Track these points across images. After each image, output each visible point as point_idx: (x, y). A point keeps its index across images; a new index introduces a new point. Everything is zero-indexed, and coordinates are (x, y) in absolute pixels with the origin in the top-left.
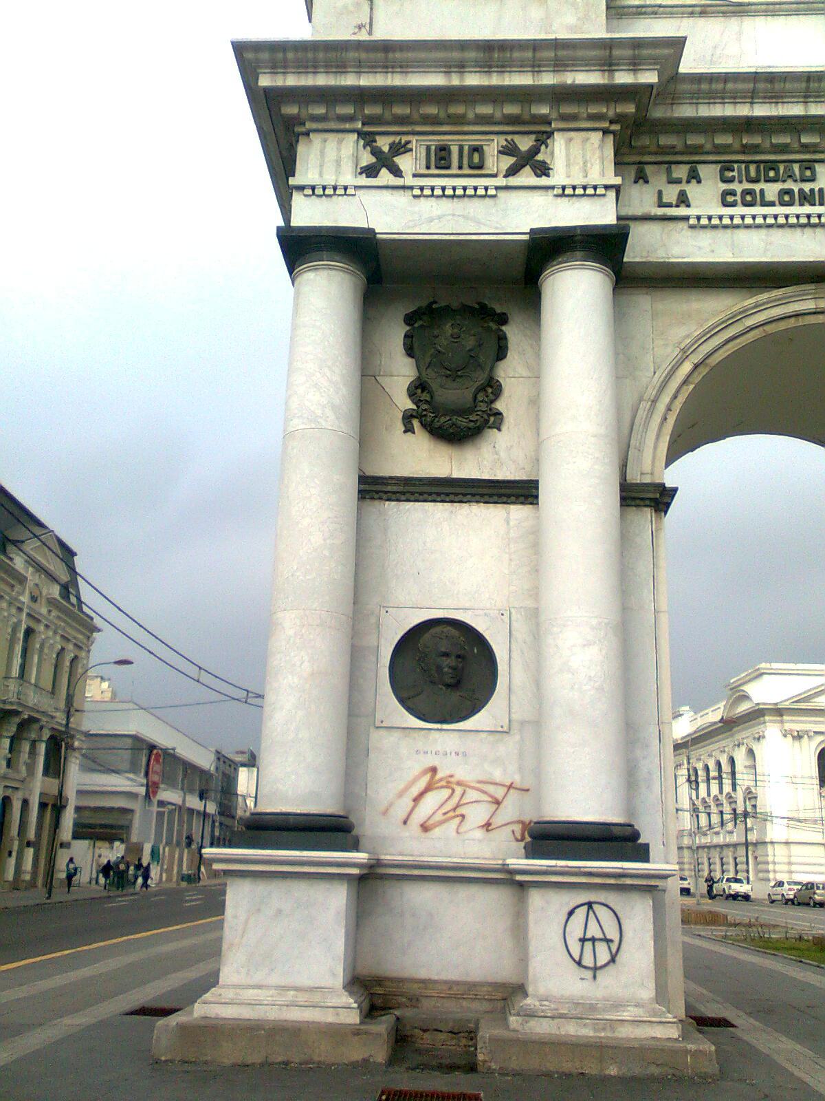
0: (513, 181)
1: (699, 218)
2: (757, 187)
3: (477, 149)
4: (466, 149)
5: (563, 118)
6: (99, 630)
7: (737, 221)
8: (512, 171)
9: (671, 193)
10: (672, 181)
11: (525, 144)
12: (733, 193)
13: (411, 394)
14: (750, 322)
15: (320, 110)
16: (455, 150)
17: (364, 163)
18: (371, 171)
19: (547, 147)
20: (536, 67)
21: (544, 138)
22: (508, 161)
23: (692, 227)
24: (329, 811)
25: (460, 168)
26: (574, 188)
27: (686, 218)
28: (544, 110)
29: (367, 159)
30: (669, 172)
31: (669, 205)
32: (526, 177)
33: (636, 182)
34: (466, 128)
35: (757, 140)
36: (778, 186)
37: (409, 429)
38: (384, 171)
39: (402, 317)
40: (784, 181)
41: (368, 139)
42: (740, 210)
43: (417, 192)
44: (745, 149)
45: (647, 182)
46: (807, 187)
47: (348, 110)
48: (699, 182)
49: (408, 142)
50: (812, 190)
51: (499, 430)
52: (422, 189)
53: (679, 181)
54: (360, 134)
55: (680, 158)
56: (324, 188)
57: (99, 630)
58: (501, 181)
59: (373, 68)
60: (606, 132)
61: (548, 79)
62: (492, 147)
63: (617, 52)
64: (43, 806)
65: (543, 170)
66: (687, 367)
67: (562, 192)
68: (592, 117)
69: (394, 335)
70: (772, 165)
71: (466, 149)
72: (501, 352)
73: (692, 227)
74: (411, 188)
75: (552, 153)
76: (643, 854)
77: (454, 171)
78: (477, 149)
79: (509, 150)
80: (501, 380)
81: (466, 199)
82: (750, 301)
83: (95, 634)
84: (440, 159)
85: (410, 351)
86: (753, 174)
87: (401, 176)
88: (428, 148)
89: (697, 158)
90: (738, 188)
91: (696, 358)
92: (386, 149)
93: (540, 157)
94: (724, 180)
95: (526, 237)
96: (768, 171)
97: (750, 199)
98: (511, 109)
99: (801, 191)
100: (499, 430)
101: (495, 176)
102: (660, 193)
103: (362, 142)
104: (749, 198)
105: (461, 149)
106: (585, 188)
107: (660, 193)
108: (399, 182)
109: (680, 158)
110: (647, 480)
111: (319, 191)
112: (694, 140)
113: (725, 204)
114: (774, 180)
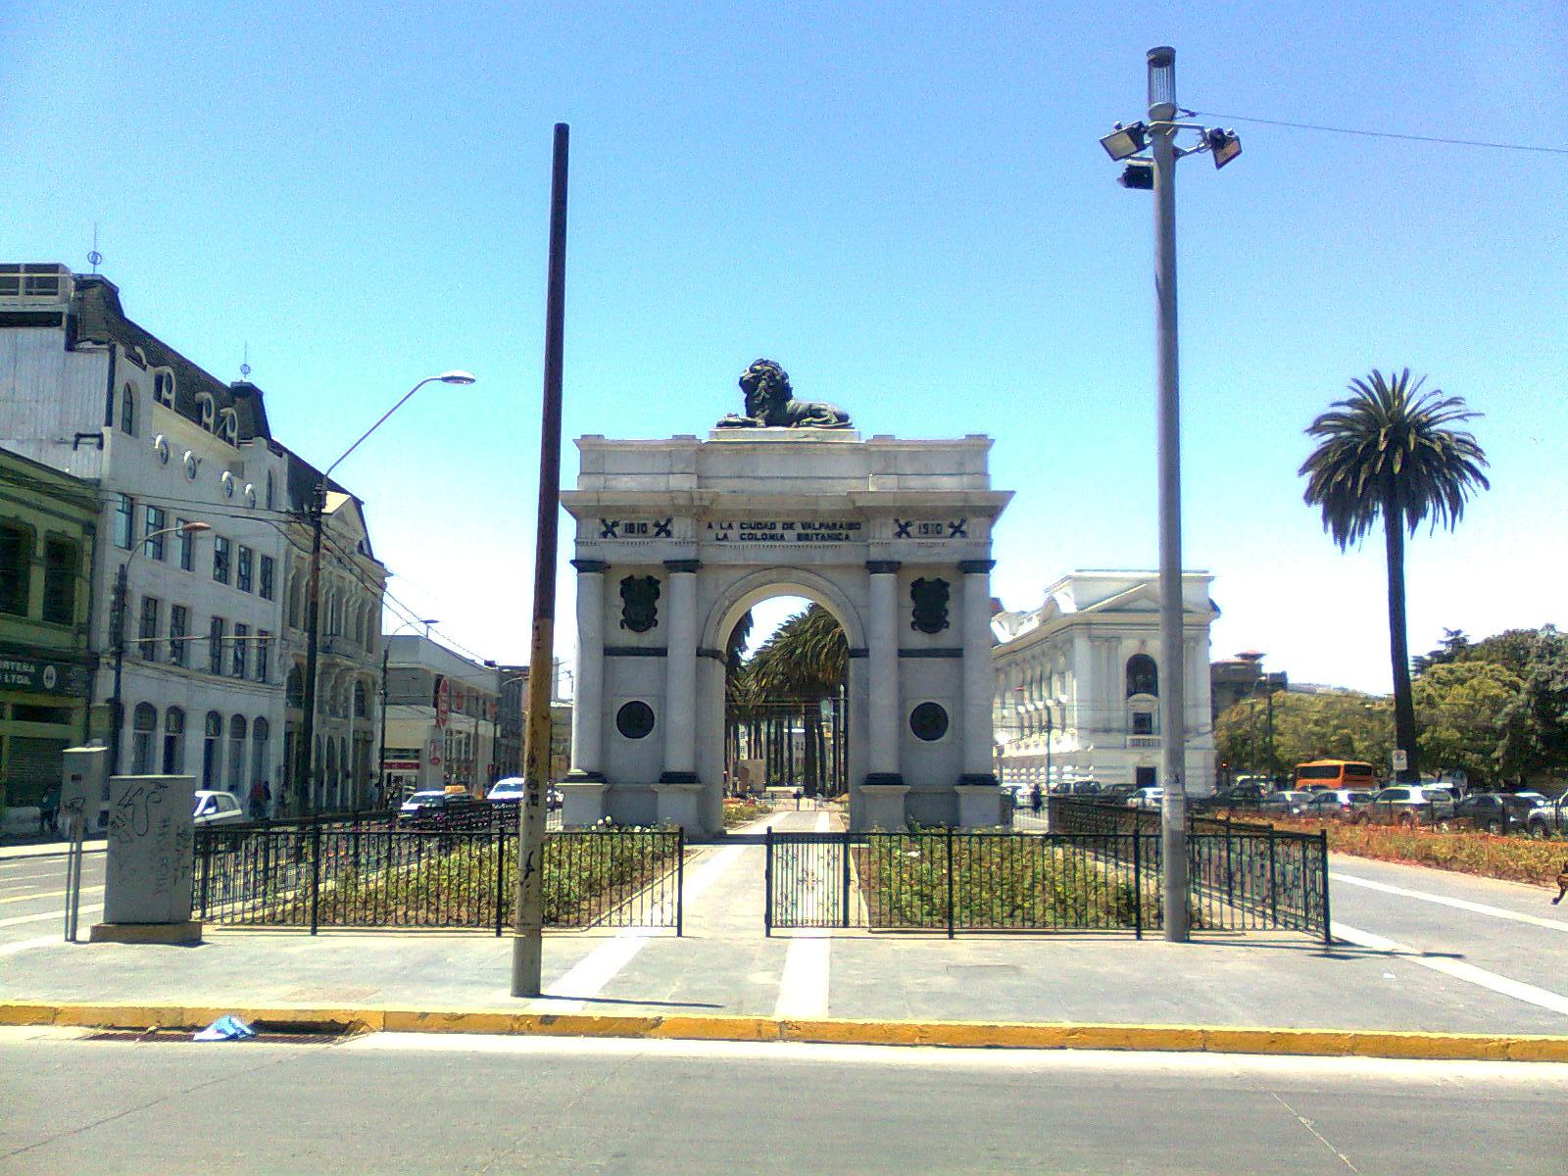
2: (753, 532)
3: (645, 525)
6: (390, 575)
10: (722, 528)
13: (623, 613)
16: (636, 526)
18: (605, 535)
36: (762, 531)
37: (622, 627)
38: (609, 535)
46: (773, 532)
57: (390, 575)
64: (356, 741)
65: (669, 534)
72: (657, 594)
75: (672, 527)
90: (746, 531)
93: (669, 528)
94: (742, 528)
97: (752, 537)
114: (761, 528)
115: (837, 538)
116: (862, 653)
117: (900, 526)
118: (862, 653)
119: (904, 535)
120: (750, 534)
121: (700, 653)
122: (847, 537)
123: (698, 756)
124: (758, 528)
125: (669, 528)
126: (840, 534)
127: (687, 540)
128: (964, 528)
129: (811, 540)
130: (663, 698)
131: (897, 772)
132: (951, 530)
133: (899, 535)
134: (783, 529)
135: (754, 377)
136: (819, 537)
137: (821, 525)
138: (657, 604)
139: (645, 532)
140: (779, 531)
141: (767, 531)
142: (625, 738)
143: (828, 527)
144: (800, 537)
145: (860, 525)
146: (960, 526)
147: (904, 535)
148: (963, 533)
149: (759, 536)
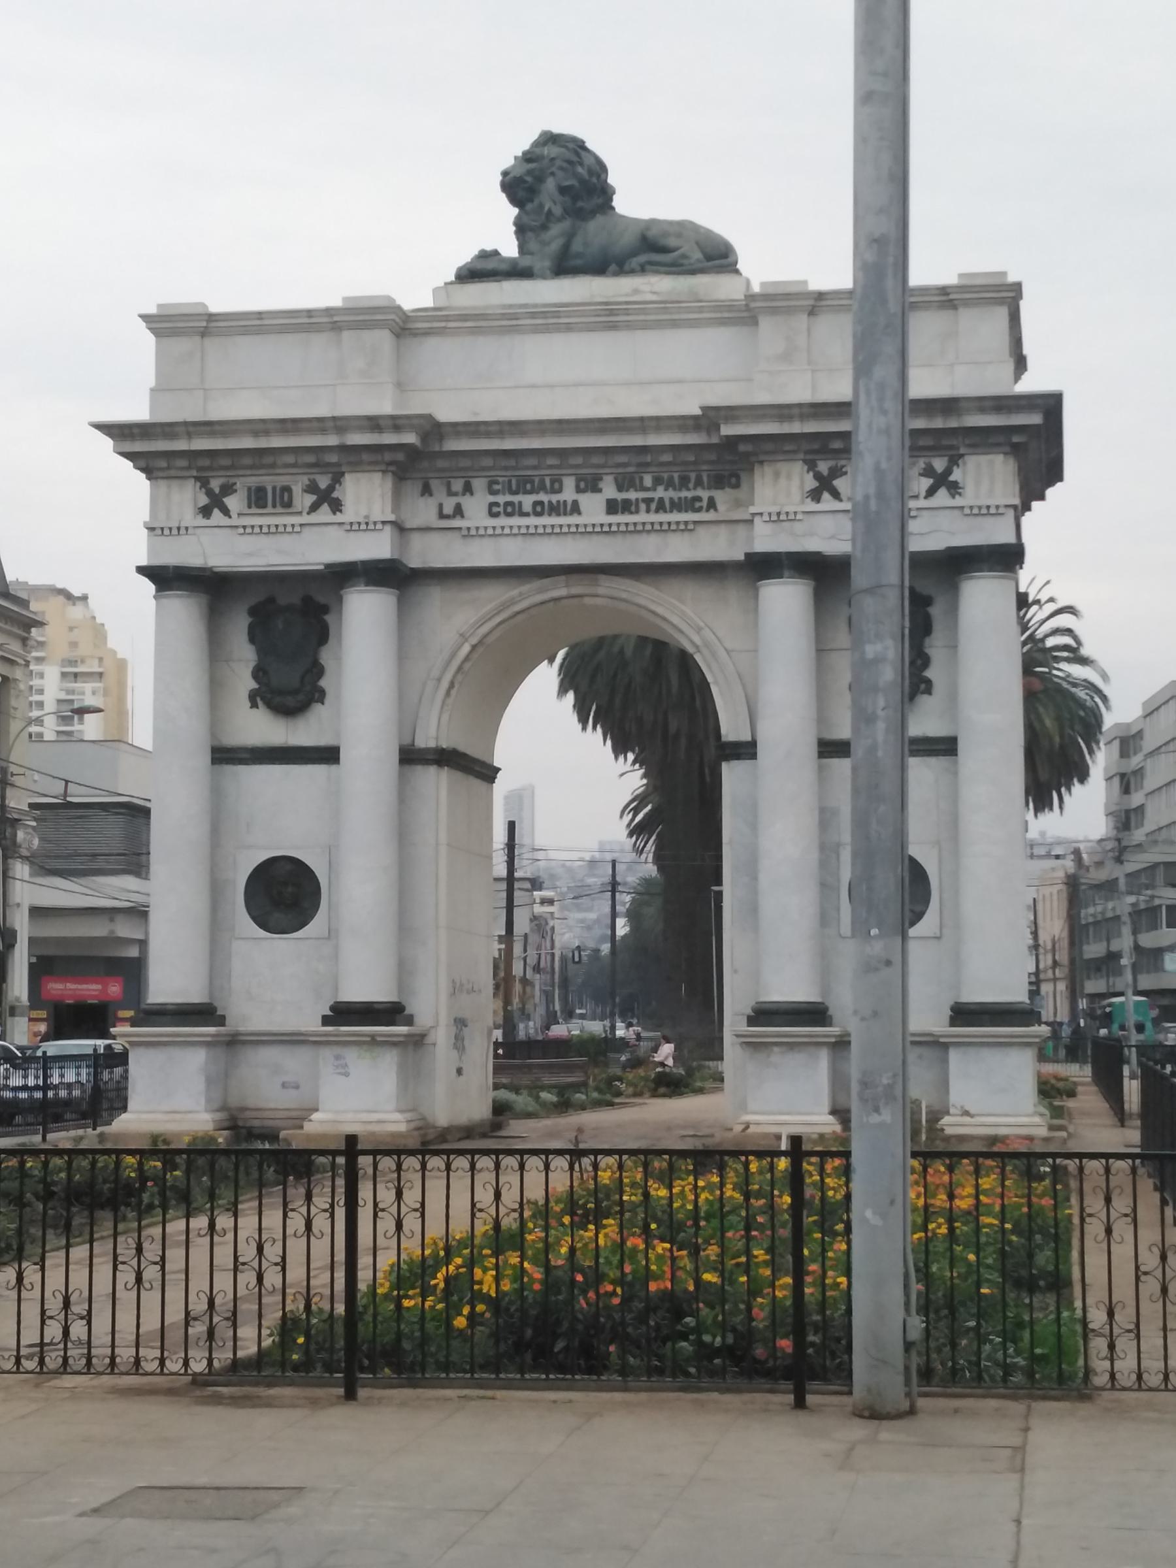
0: (315, 518)
1: (469, 529)
4: (278, 489)
5: (350, 463)
7: (499, 531)
8: (314, 508)
9: (448, 509)
10: (450, 493)
11: (323, 482)
12: (497, 504)
14: (517, 608)
15: (164, 464)
17: (201, 504)
18: (206, 512)
19: (340, 484)
20: (323, 431)
21: (337, 478)
22: (310, 499)
23: (464, 536)
24: (196, 1000)
25: (274, 506)
26: (359, 524)
27: (460, 529)
28: (333, 458)
29: (204, 500)
30: (449, 485)
31: (448, 517)
32: (324, 514)
33: (423, 495)
34: (278, 471)
35: (512, 463)
37: (254, 705)
38: (216, 512)
39: (246, 607)
40: (538, 493)
41: (204, 483)
42: (503, 521)
43: (241, 530)
44: (506, 468)
45: (431, 495)
46: (555, 498)
47: (183, 463)
48: (472, 494)
49: (235, 484)
50: (558, 502)
51: (323, 704)
52: (244, 527)
53: (456, 494)
54: (197, 478)
55: (455, 474)
56: (170, 529)
58: (305, 519)
59: (201, 435)
60: (384, 472)
61: (332, 440)
62: (297, 490)
63: (382, 422)
66: (466, 648)
67: (353, 528)
68: (371, 463)
69: (238, 626)
70: (529, 480)
71: (278, 489)
72: (322, 635)
73: (464, 536)
74: (237, 527)
76: (409, 1021)
77: (269, 510)
78: (287, 489)
79: (312, 488)
80: (322, 662)
81: (278, 535)
82: (515, 592)
83: (34, 631)
84: (258, 498)
85: (252, 639)
86: (514, 487)
87: (230, 517)
88: (249, 489)
89: (470, 474)
90: (501, 499)
91: (474, 641)
92: (217, 491)
93: (335, 495)
94: (493, 492)
95: (322, 567)
96: (524, 486)
97: (513, 510)
98: (311, 459)
99: (550, 502)
100: (323, 704)
101: (300, 513)
102: (441, 506)
103: (198, 484)
104: (509, 509)
105: (274, 489)
106: (367, 524)
107: (441, 506)
108: (225, 521)
109: (455, 474)
110: (432, 744)
111: (166, 532)
112: (465, 463)
113: (493, 515)
115: (690, 505)
116: (746, 750)
117: (818, 476)
118: (746, 750)
119: (826, 496)
120: (507, 504)
121: (410, 756)
122: (712, 505)
123: (404, 971)
124: (526, 492)
125: (335, 495)
126: (699, 499)
127: (373, 518)
128: (956, 475)
129: (637, 512)
130: (331, 851)
131: (819, 1000)
132: (926, 483)
133: (815, 495)
134: (579, 490)
135: (529, 172)
136: (653, 506)
137: (657, 481)
138: (326, 656)
139: (289, 504)
140: (568, 494)
141: (543, 497)
142: (262, 933)
143: (670, 484)
144: (612, 507)
145: (738, 477)
146: (948, 471)
147: (826, 496)
148: (954, 489)
149: (527, 505)
